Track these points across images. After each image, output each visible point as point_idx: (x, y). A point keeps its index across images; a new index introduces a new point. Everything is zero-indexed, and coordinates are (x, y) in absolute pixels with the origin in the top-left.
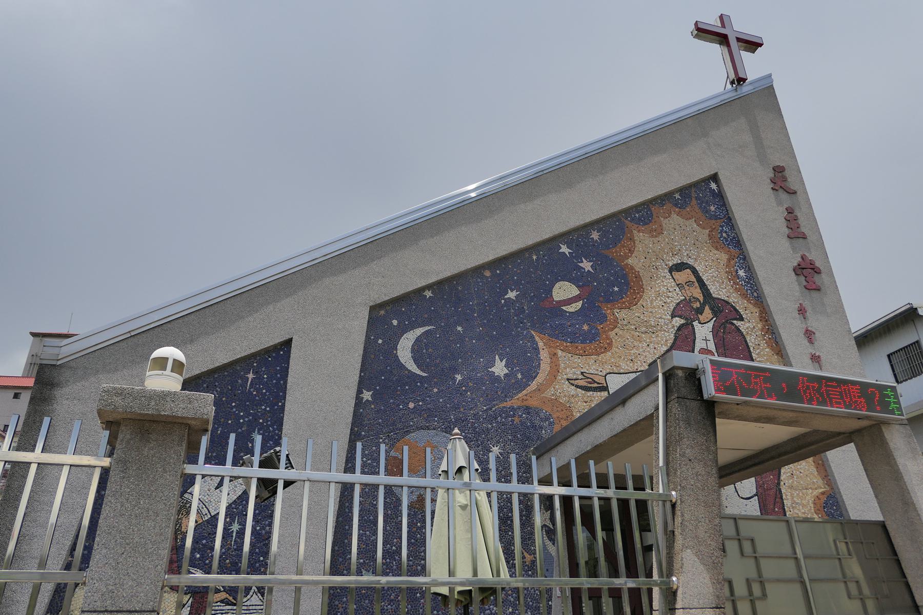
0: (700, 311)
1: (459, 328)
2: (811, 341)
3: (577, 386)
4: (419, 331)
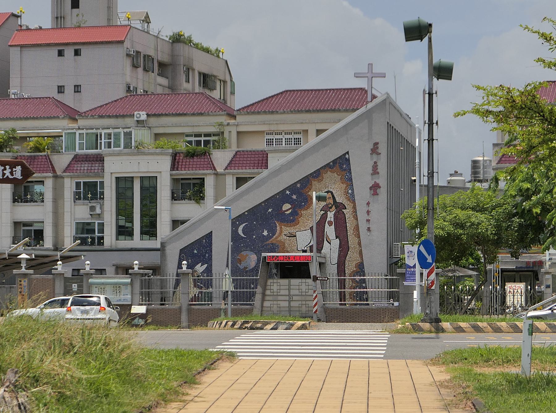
0: (331, 208)
1: (255, 223)
2: (368, 214)
3: (287, 236)
4: (244, 225)
